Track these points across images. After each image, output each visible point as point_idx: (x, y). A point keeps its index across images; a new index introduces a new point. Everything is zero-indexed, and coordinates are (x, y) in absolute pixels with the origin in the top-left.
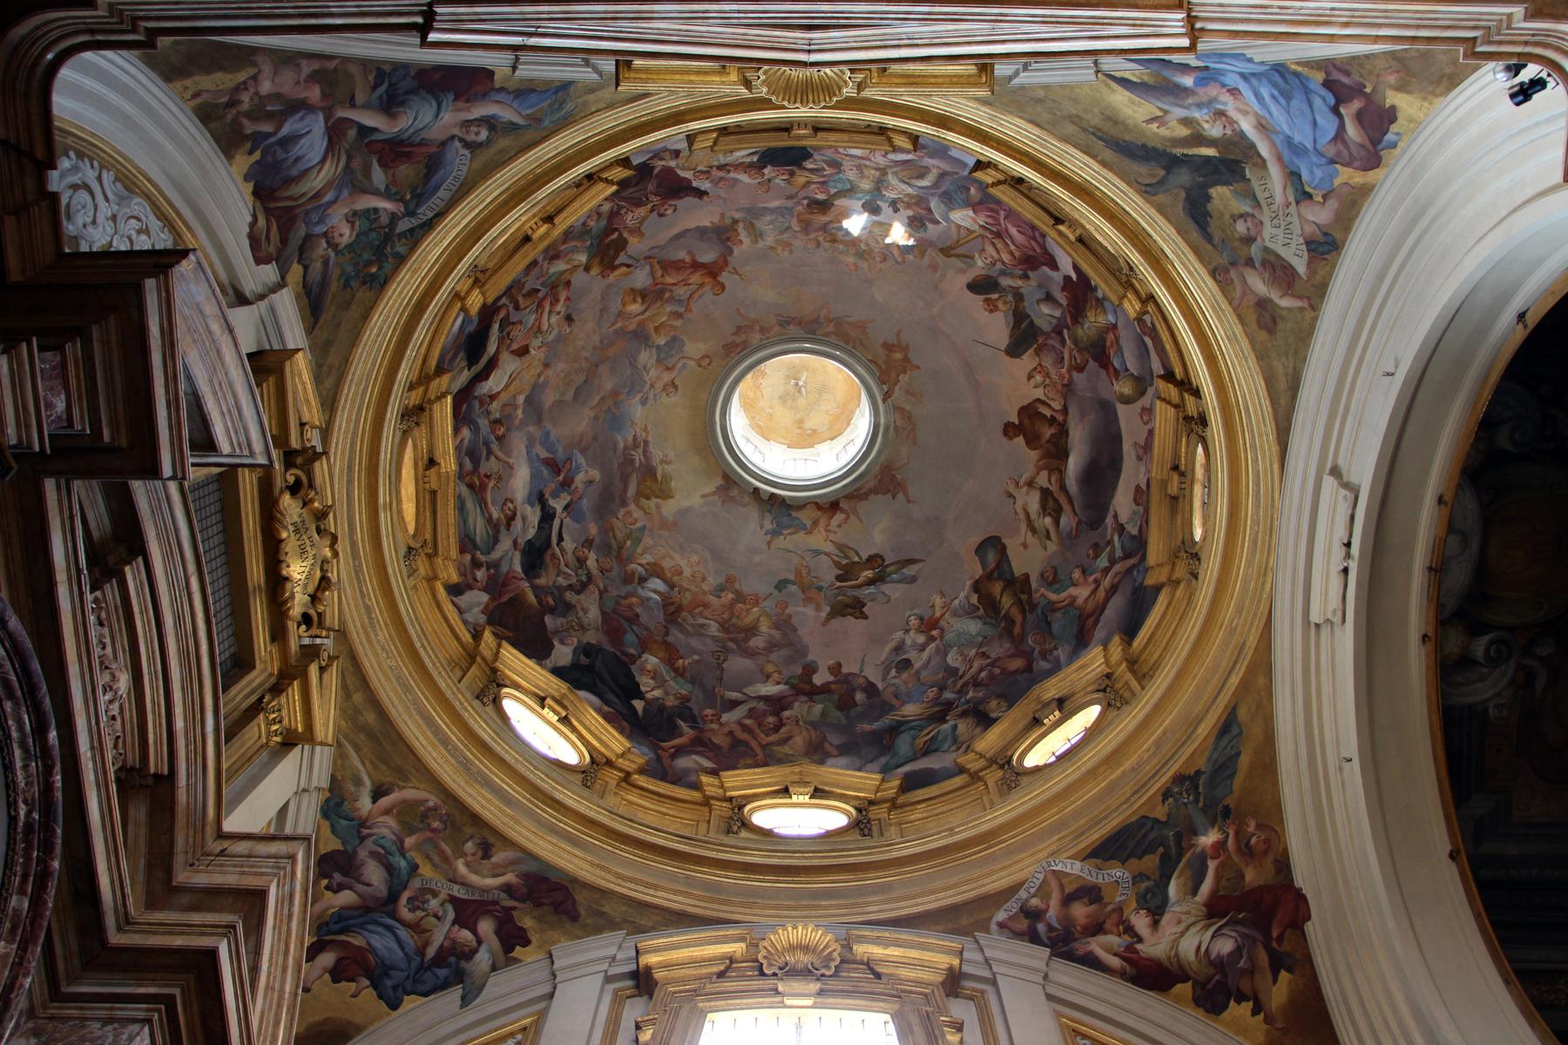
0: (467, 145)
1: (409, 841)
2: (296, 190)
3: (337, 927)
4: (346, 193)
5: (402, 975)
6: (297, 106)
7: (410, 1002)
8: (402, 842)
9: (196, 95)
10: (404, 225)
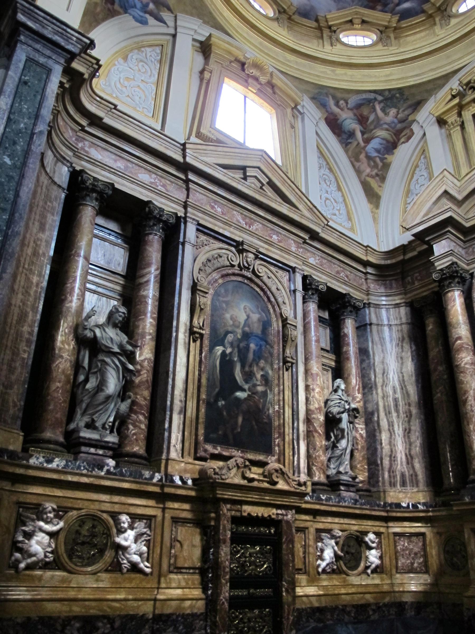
0: (347, 103)
2: (389, 137)
4: (382, 122)
6: (369, 158)
9: (380, 186)
10: (380, 98)
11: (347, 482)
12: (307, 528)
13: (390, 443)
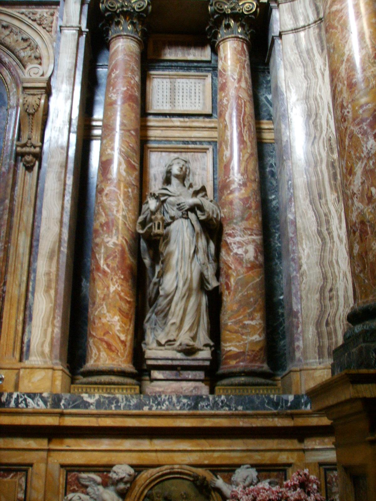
11: (169, 363)
12: (31, 465)
13: (321, 263)
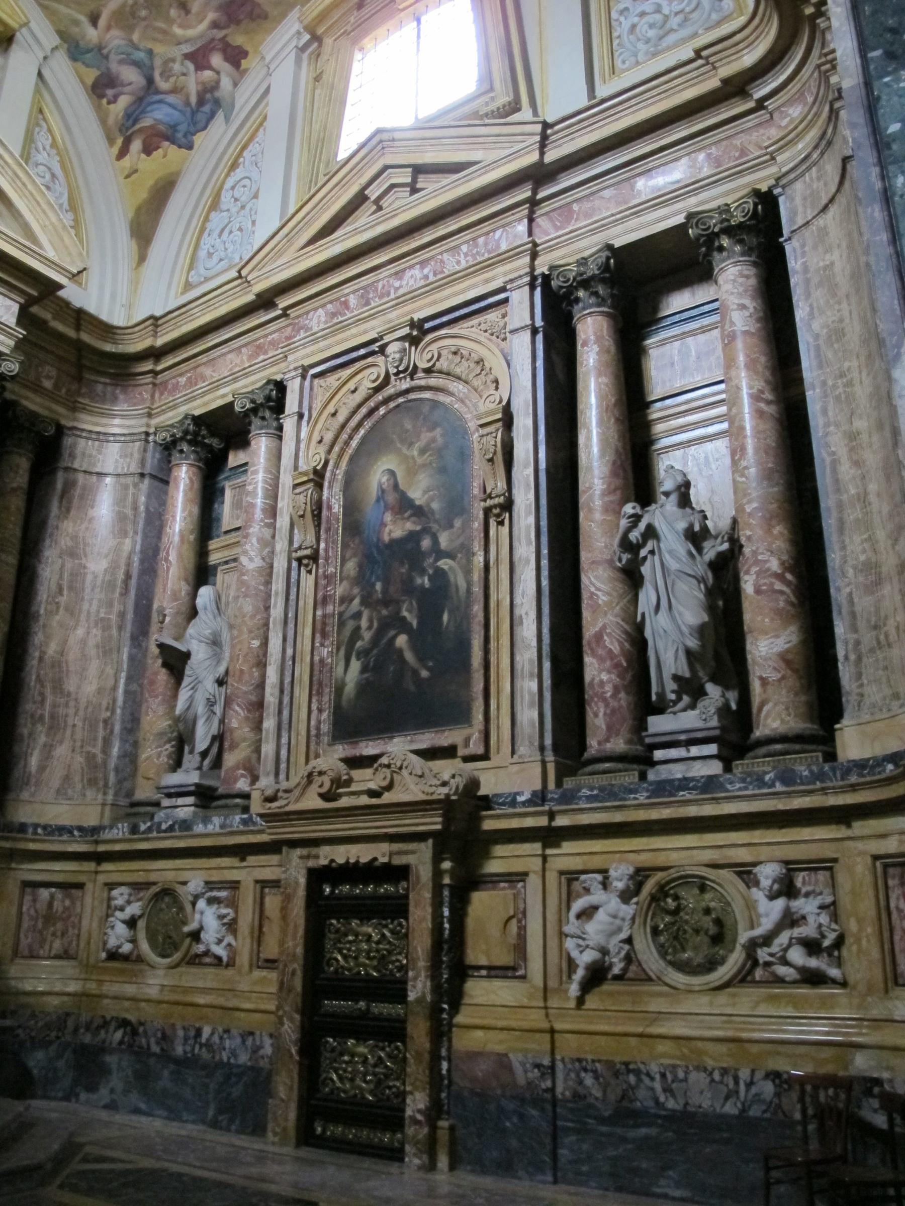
1: (135, 37)
3: (130, 122)
5: (185, 125)
7: (198, 139)
8: (131, 41)
